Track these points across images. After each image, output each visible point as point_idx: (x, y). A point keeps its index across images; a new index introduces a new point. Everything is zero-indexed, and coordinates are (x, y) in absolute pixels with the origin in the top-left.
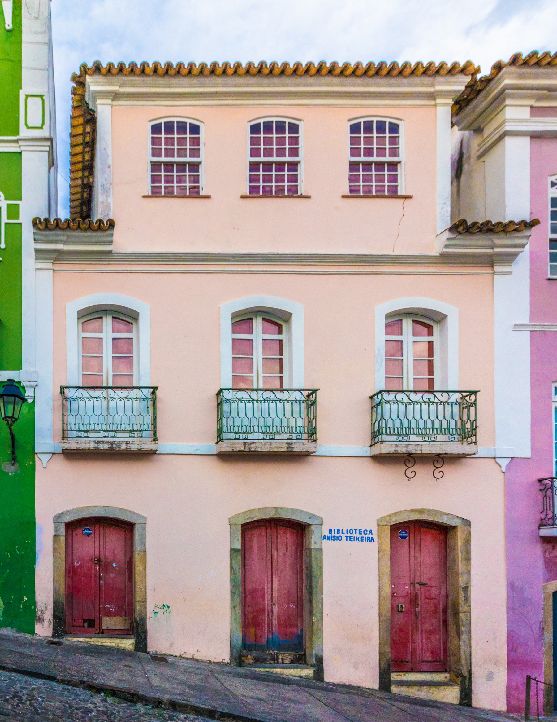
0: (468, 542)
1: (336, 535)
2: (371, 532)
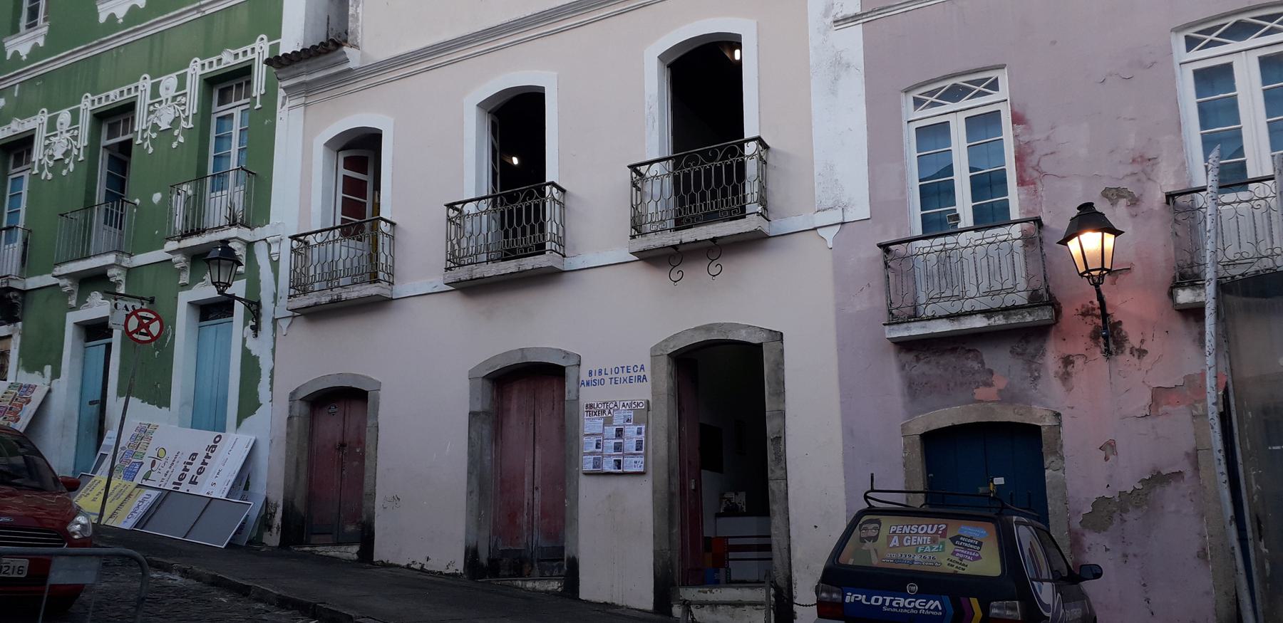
0: (779, 365)
1: (598, 377)
2: (642, 368)
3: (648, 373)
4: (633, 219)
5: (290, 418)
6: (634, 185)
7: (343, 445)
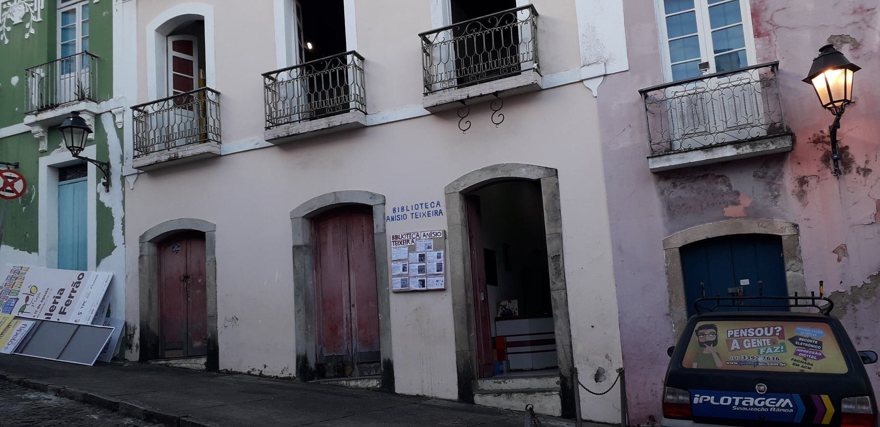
0: (556, 196)
1: (401, 213)
2: (438, 204)
3: (443, 208)
4: (425, 81)
5: (141, 257)
6: (425, 51)
7: (186, 277)
